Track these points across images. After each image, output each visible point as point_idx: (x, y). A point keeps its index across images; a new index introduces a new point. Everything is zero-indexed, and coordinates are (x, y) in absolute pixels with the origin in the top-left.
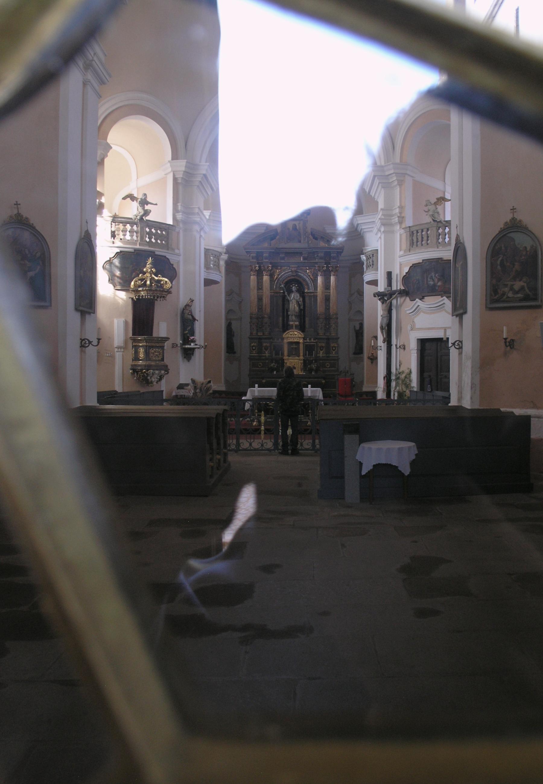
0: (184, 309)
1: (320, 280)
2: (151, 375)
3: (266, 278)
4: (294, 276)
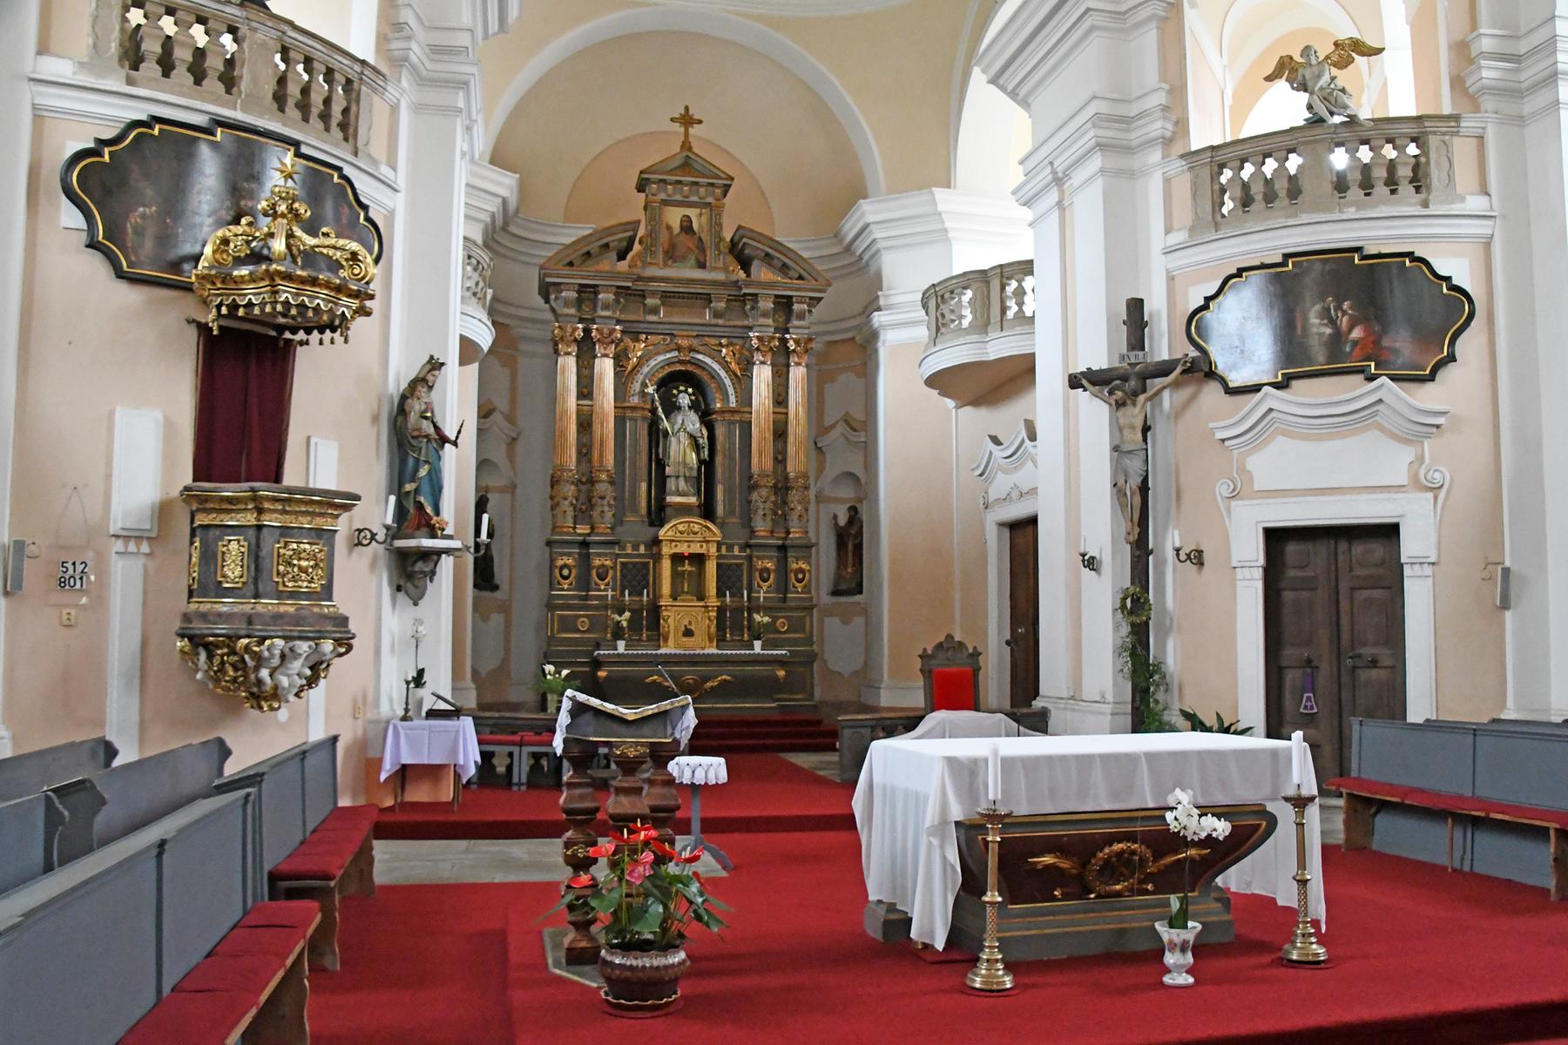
0: (404, 398)
1: (762, 376)
2: (276, 662)
3: (605, 367)
4: (681, 362)
